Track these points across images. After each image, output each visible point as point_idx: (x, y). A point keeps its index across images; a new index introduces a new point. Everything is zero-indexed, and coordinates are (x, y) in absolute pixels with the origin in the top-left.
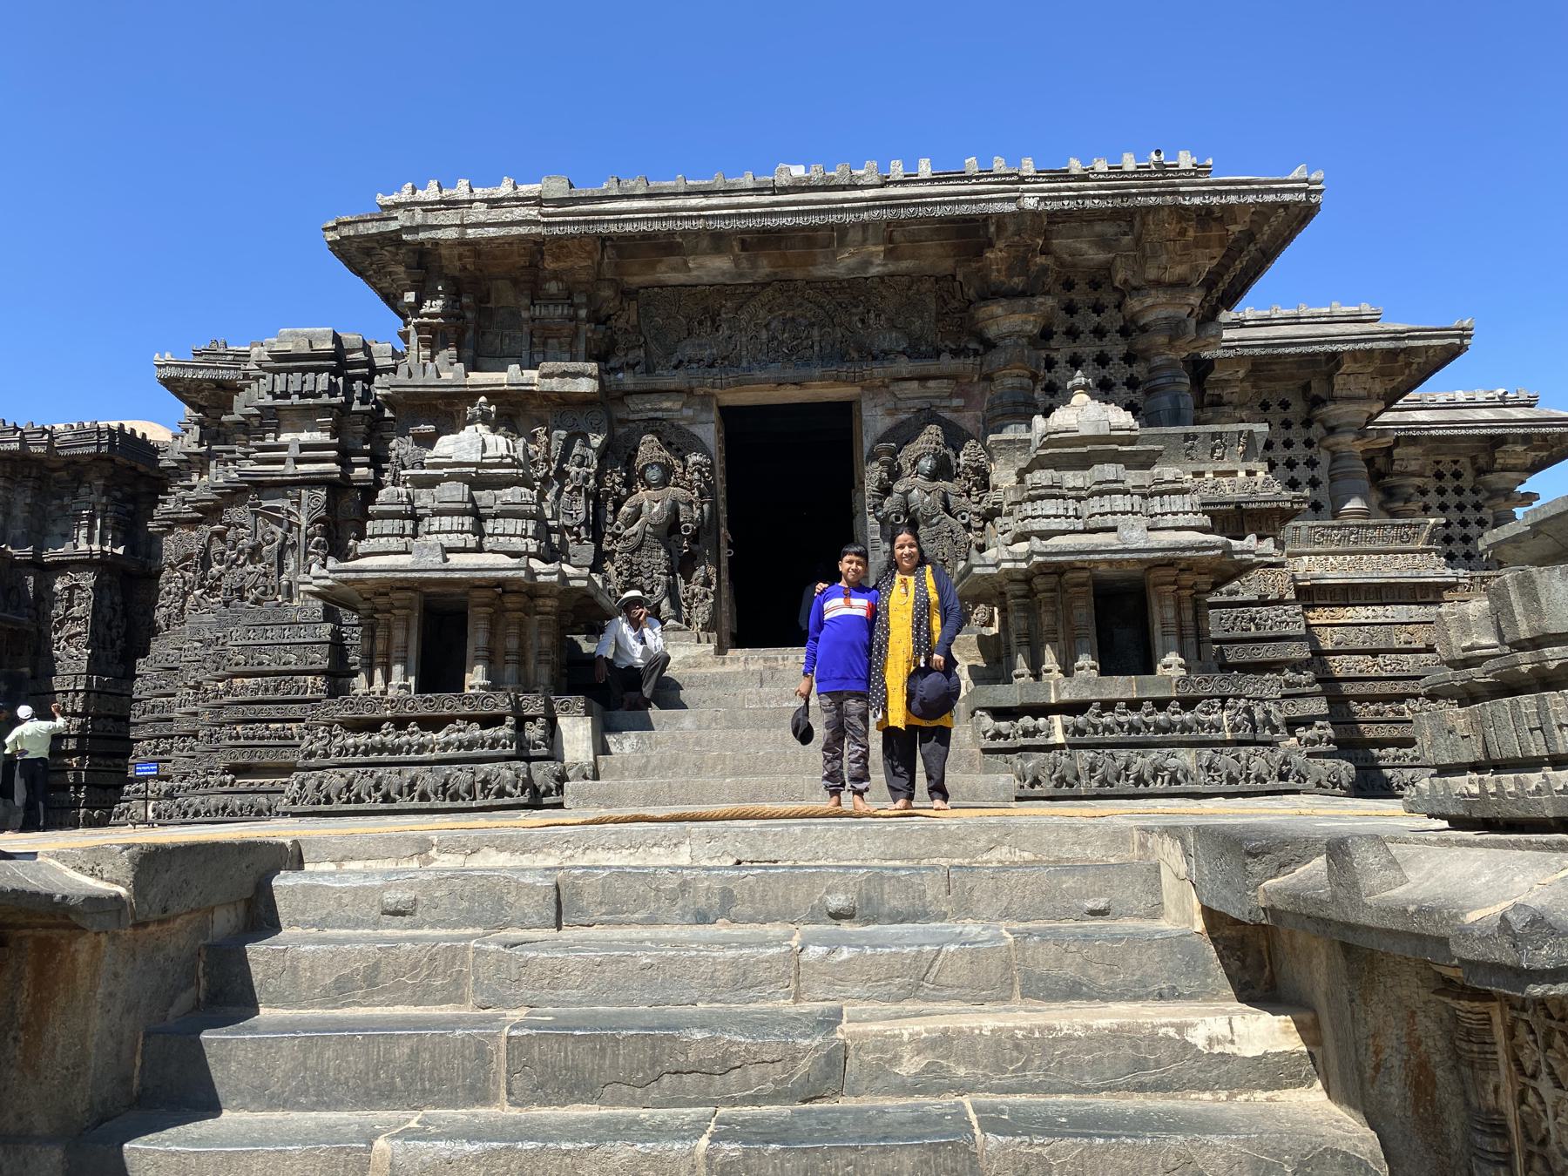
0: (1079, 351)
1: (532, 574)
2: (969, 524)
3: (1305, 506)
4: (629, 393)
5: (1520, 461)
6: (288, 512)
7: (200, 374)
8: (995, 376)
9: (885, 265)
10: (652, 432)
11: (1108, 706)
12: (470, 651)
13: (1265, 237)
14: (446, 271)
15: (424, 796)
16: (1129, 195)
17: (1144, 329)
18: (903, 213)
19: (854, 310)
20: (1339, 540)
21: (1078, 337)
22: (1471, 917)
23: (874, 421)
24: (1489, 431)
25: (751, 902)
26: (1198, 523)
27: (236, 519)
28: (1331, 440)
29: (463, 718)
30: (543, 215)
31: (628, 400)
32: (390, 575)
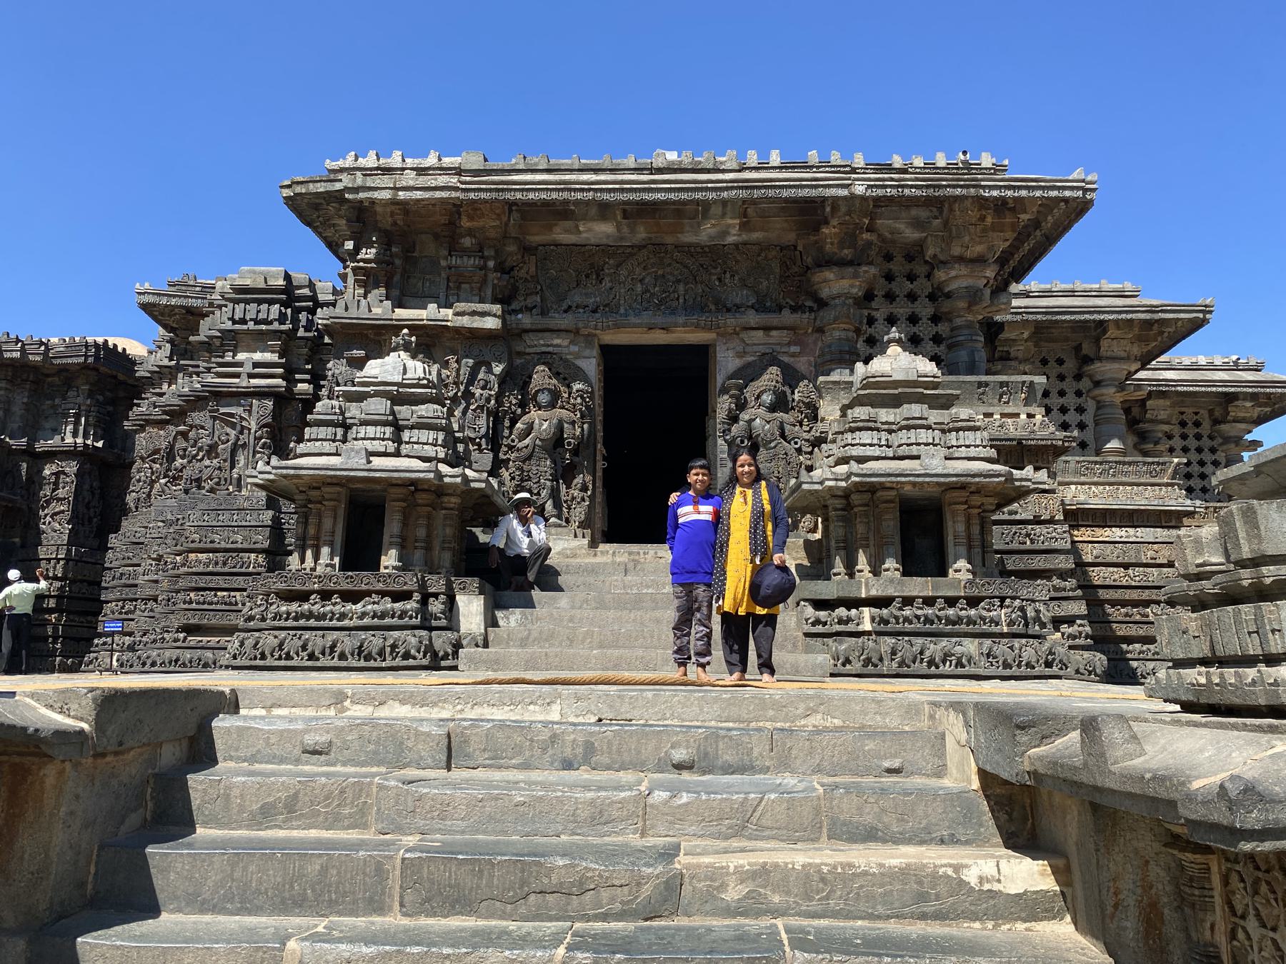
0: (895, 311)
1: (440, 476)
2: (800, 448)
3: (1074, 444)
5: (1249, 415)
6: (241, 418)
7: (173, 301)
8: (826, 329)
9: (739, 235)
11: (908, 601)
12: (386, 538)
13: (1049, 225)
15: (342, 656)
16: (940, 187)
17: (948, 296)
18: (756, 194)
19: (713, 271)
20: (1101, 473)
21: (894, 300)
22: (1196, 785)
23: (726, 362)
24: (1224, 389)
25: (609, 753)
26: (986, 455)
27: (198, 422)
28: (1097, 392)
29: (377, 592)
31: (525, 337)
32: (322, 472)
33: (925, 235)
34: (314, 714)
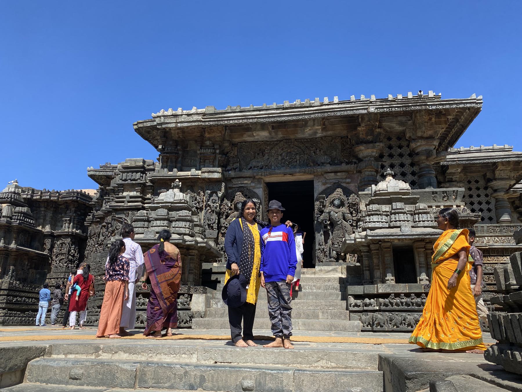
0: (394, 162)
1: (185, 241)
3: (480, 219)
4: (233, 178)
6: (125, 219)
7: (101, 173)
8: (362, 171)
9: (322, 133)
10: (240, 191)
11: (397, 295)
13: (462, 120)
14: (173, 138)
16: (409, 106)
17: (417, 154)
18: (326, 115)
19: (312, 149)
21: (393, 157)
23: (319, 187)
25: (212, 382)
26: (432, 225)
28: (495, 195)
30: (203, 119)
31: (233, 180)
33: (405, 128)
34: (86, 358)
